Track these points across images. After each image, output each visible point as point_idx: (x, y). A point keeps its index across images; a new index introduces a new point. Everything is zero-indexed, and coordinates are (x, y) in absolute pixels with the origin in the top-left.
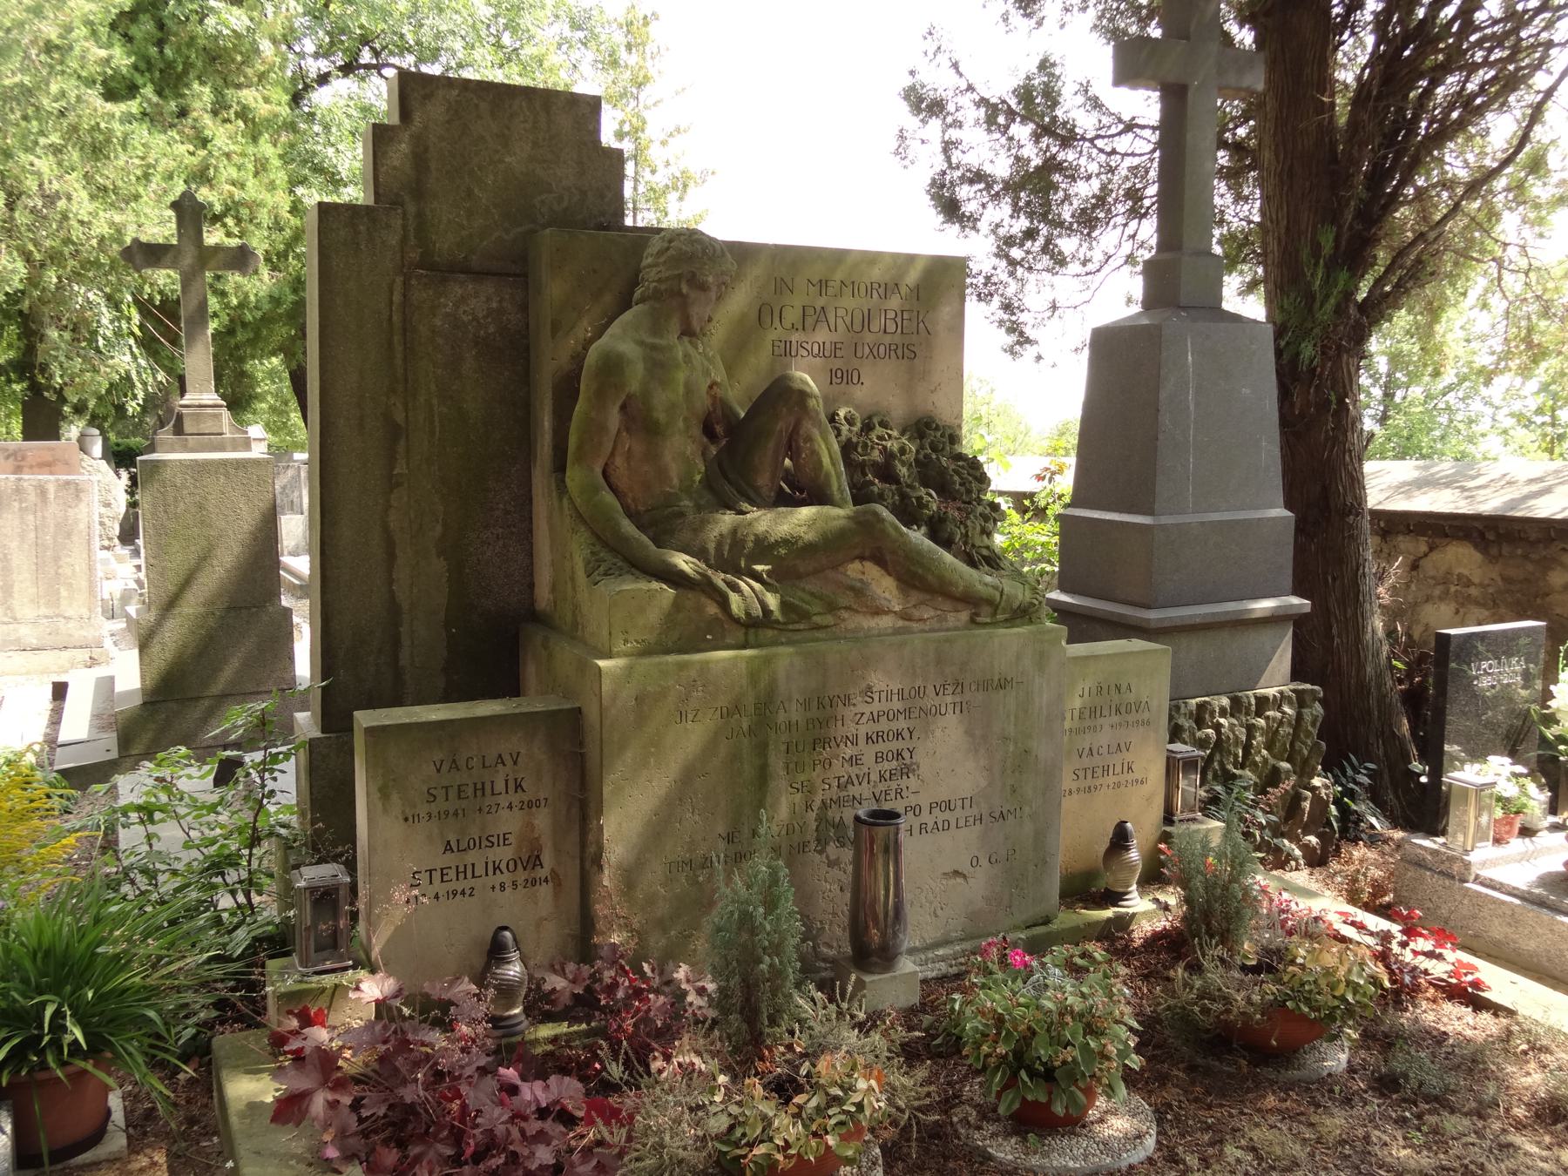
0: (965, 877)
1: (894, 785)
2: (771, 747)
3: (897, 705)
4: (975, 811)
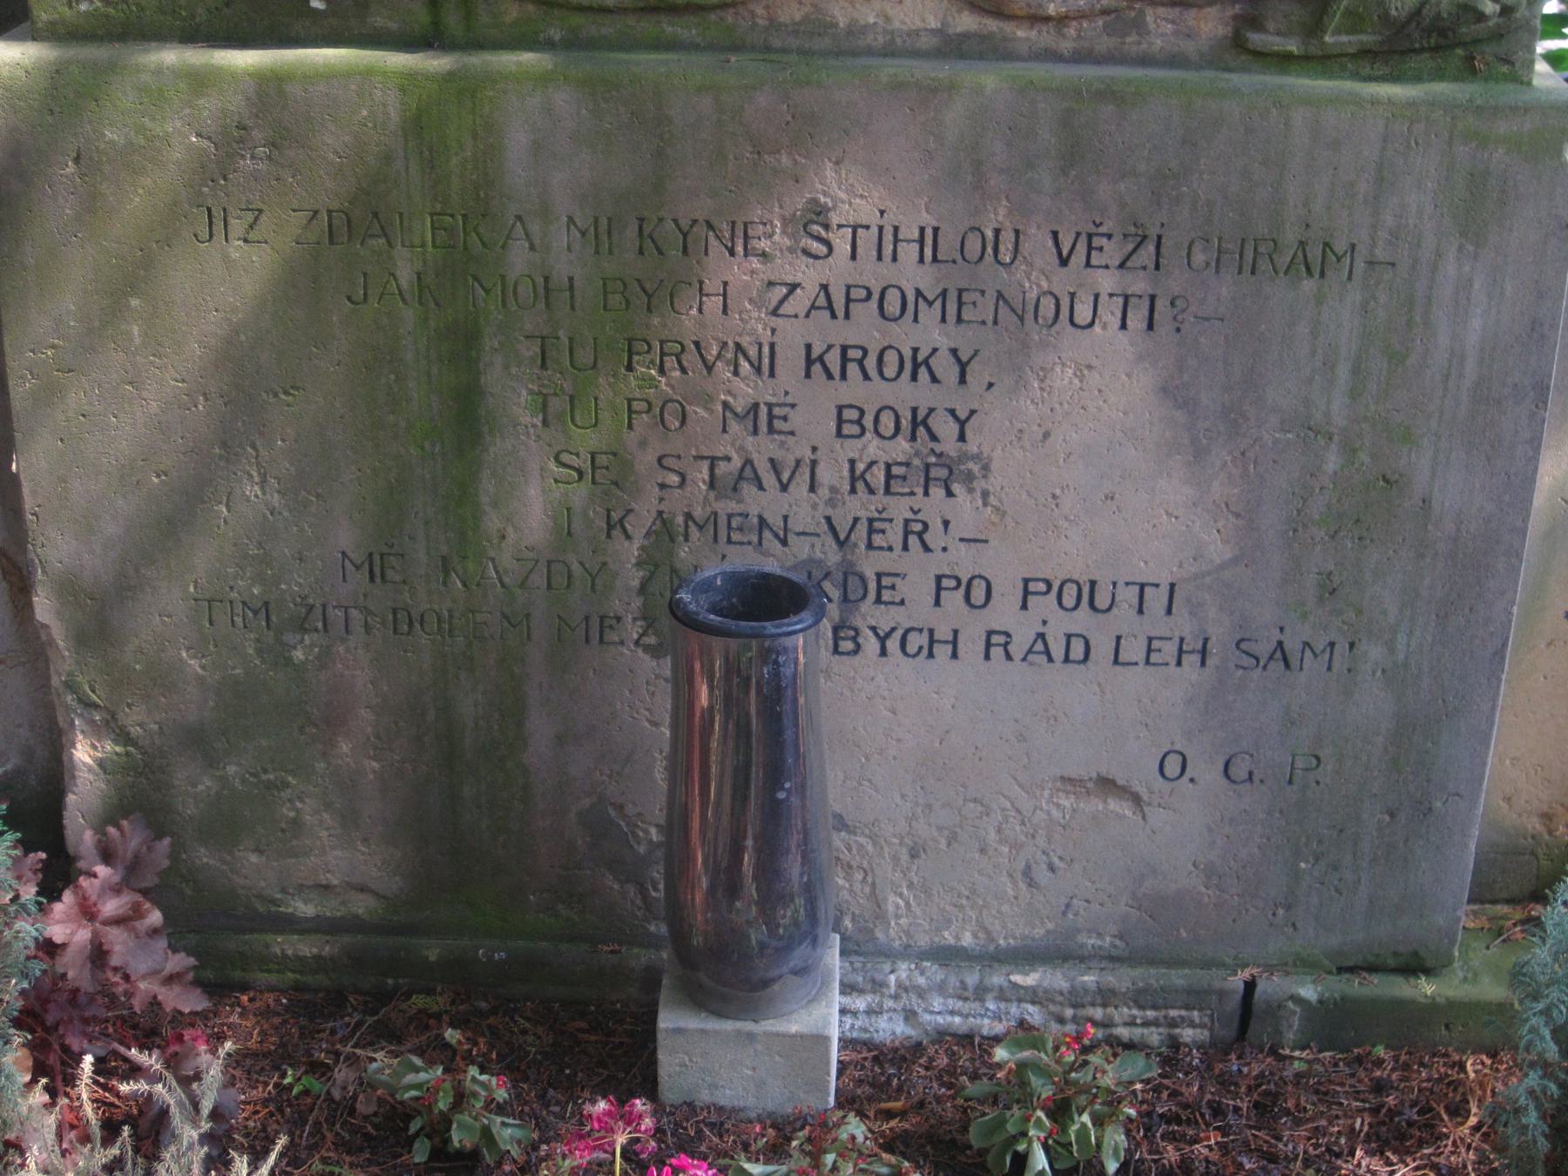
0: (1136, 799)
1: (899, 509)
2: (490, 342)
3: (911, 274)
4: (1182, 624)
